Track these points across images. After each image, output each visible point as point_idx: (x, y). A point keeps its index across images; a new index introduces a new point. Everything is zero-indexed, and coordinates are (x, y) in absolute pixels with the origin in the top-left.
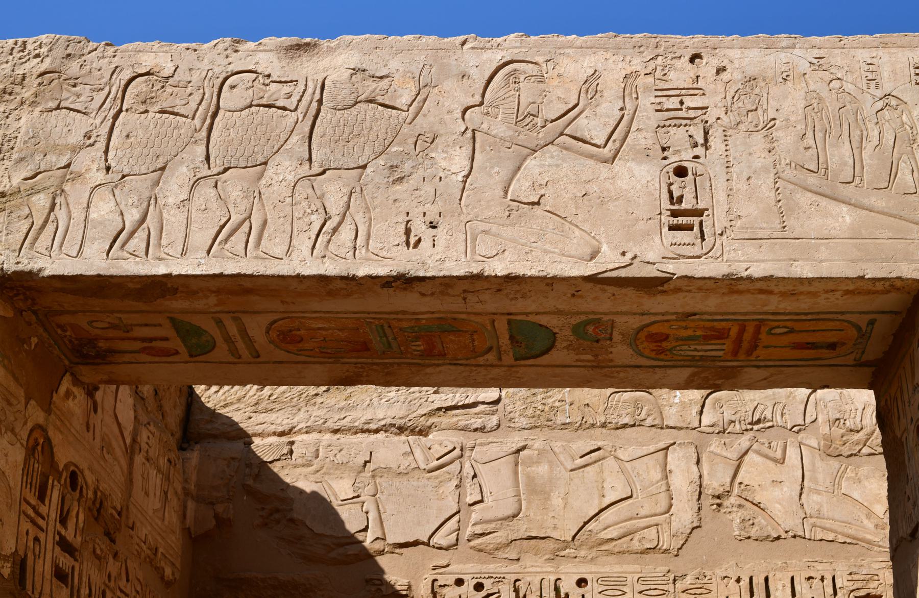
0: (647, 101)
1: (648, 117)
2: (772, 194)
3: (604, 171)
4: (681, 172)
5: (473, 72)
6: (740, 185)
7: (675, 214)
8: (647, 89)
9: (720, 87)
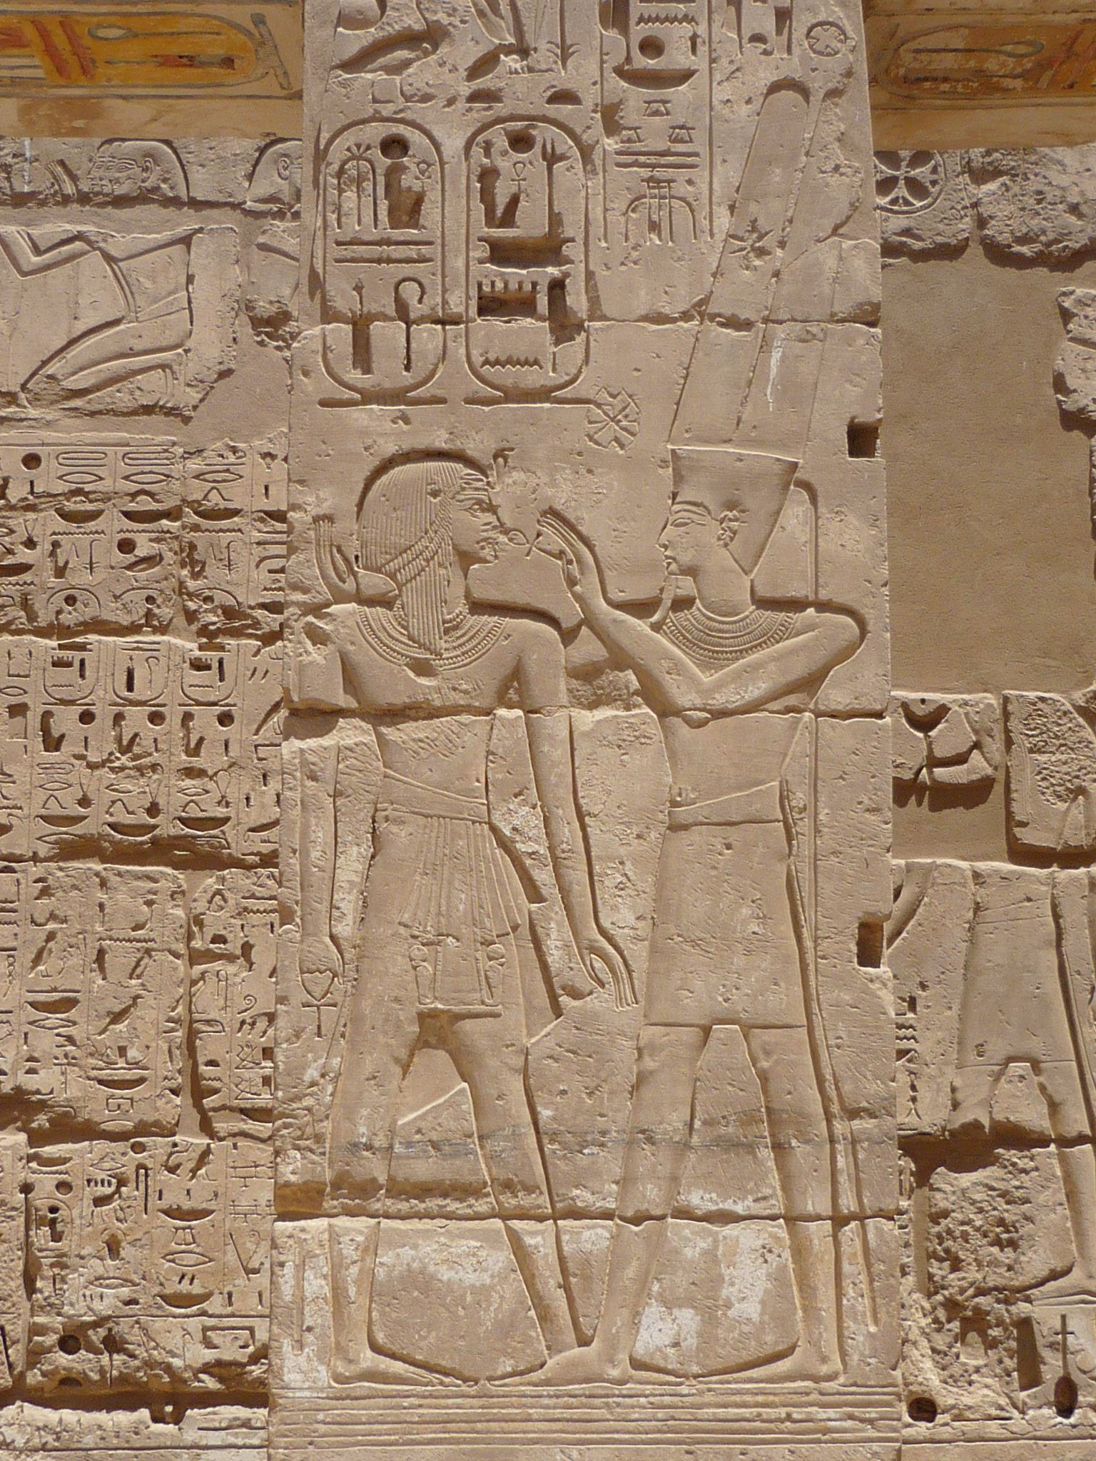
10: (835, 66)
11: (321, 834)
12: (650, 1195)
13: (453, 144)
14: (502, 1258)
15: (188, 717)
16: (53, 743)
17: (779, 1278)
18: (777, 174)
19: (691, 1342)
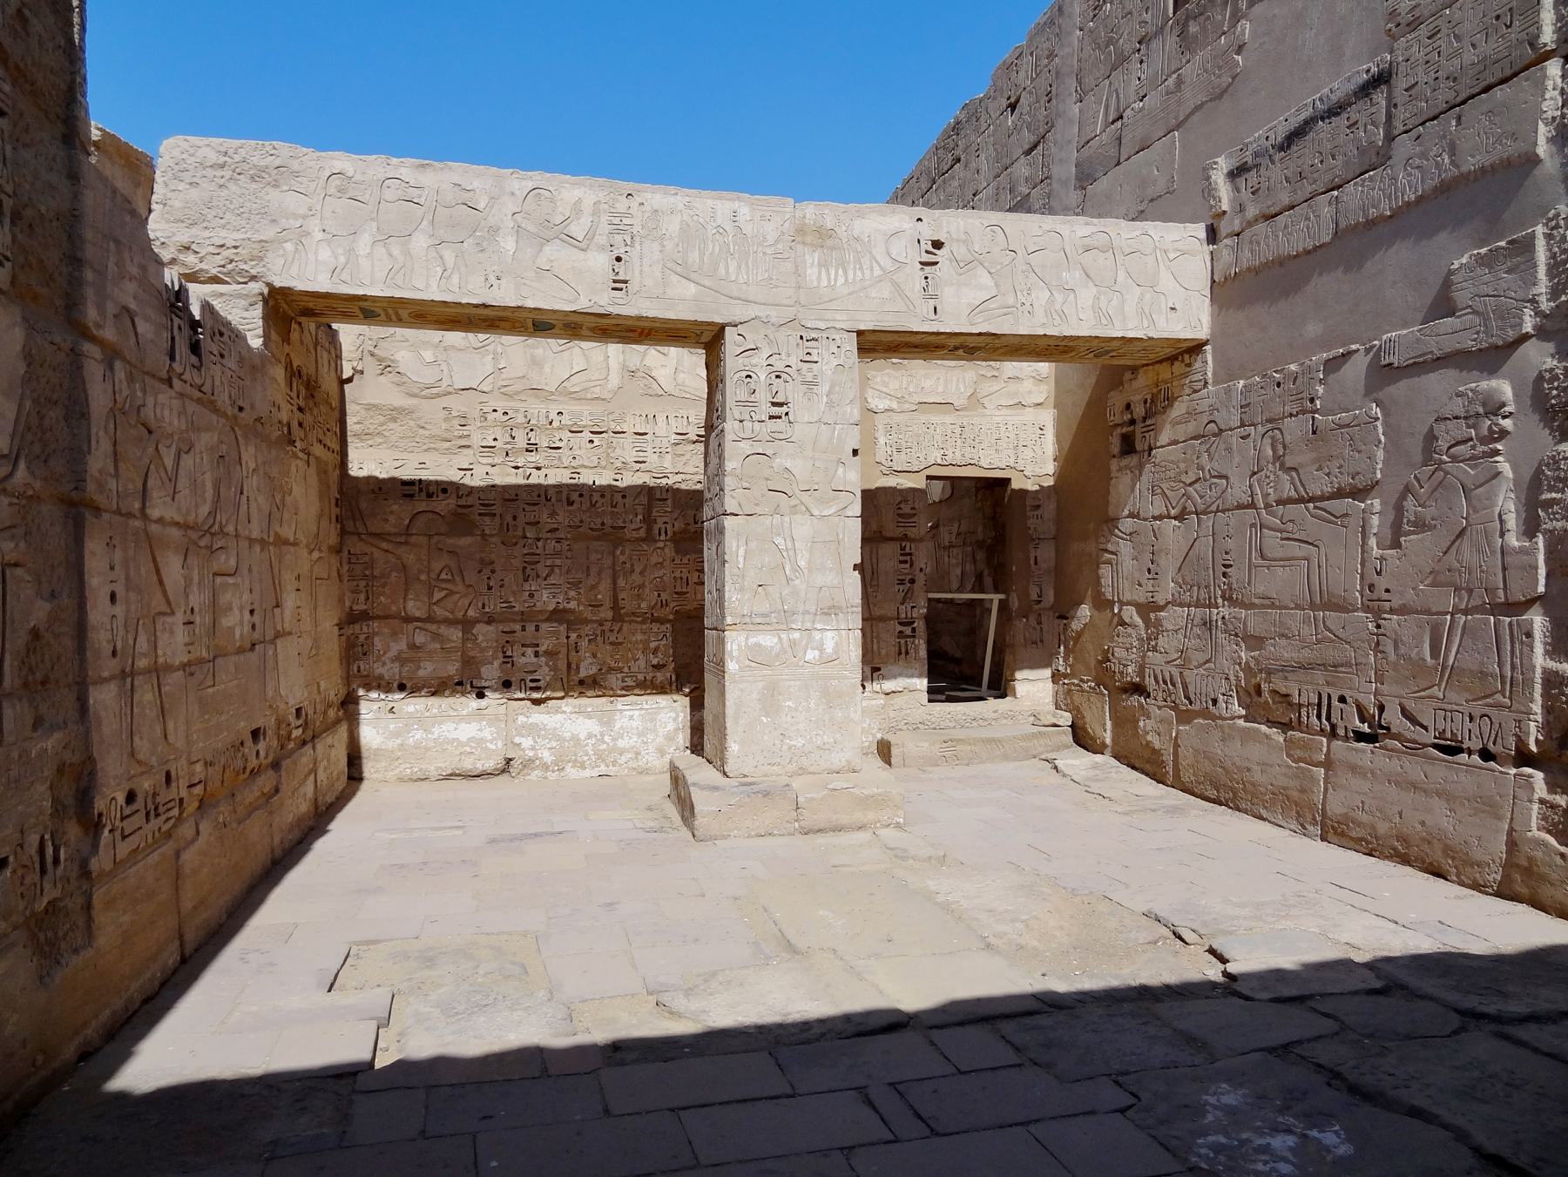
0: (605, 218)
1: (604, 228)
2: (660, 275)
3: (582, 255)
4: (619, 259)
5: (517, 192)
6: (646, 269)
7: (615, 281)
8: (605, 211)
9: (640, 214)
10: (851, 361)
11: (735, 544)
12: (808, 625)
13: (763, 377)
14: (776, 640)
15: (612, 496)
16: (571, 503)
17: (836, 644)
18: (837, 388)
19: (817, 658)
